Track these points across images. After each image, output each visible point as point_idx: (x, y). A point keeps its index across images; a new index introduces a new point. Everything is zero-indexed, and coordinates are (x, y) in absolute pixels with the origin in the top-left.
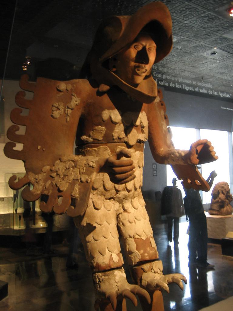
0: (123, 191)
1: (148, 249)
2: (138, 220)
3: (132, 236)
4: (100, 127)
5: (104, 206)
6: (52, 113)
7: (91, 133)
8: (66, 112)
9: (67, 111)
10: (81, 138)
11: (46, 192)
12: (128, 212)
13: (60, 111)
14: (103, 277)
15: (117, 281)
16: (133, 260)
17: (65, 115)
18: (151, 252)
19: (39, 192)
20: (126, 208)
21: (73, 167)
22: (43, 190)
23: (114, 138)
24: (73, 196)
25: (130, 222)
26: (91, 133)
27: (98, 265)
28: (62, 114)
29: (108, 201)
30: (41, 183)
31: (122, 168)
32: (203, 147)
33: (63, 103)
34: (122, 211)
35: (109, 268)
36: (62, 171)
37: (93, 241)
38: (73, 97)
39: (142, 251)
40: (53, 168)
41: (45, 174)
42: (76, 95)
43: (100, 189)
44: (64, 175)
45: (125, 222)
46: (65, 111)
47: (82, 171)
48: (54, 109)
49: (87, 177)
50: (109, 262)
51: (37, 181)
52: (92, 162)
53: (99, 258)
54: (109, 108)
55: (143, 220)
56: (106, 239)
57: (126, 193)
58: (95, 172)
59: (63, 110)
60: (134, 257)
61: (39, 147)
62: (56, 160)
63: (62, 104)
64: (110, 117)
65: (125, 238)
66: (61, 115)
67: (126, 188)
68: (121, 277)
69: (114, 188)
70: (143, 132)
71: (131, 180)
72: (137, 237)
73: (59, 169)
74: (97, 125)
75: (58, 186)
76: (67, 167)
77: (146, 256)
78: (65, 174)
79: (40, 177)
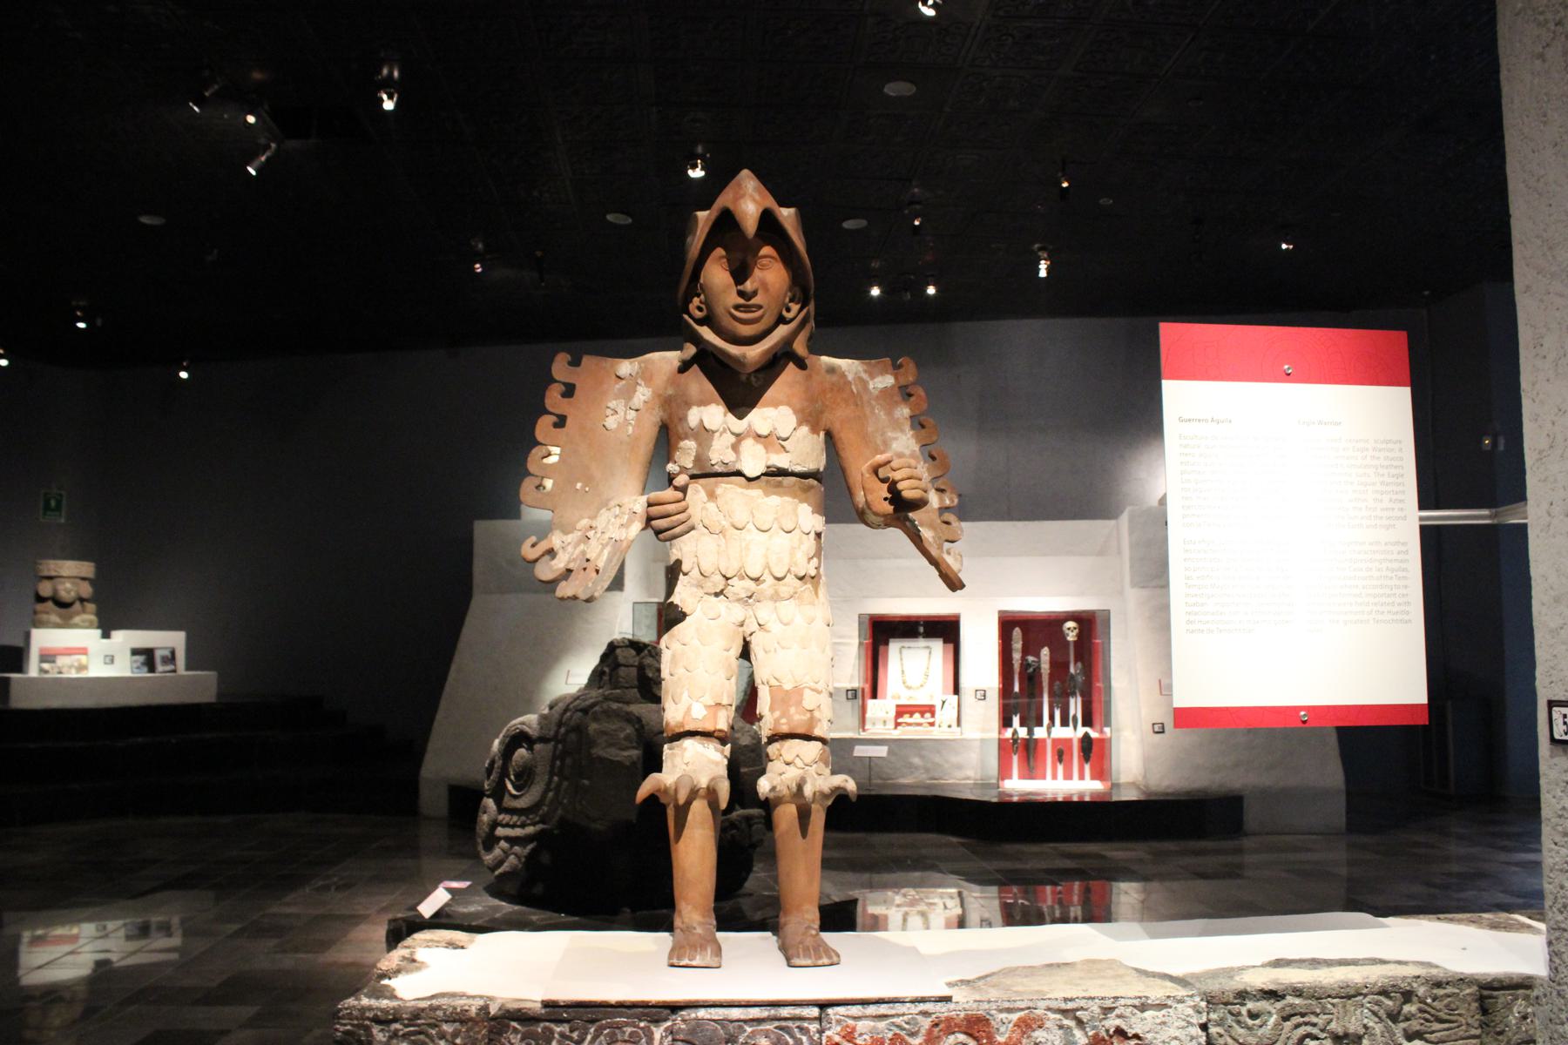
1: (793, 710)
2: (783, 648)
18: (797, 717)
22: (569, 562)
28: (621, 420)
29: (713, 599)
33: (623, 401)
38: (638, 387)
42: (643, 383)
46: (625, 414)
48: (609, 412)
50: (684, 718)
54: (703, 403)
58: (636, 522)
59: (622, 413)
61: (579, 485)
64: (701, 421)
66: (619, 423)
77: (783, 724)
79: (570, 538)
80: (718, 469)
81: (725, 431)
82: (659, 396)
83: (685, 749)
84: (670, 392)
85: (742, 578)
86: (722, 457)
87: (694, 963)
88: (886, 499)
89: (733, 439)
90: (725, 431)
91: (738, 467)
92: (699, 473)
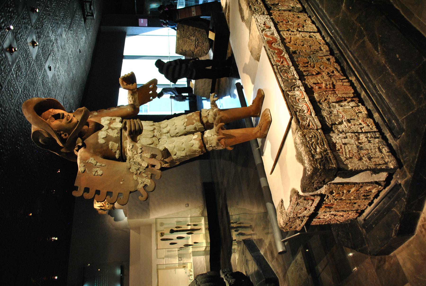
0: (154, 133)
1: (193, 117)
2: (175, 124)
3: (184, 128)
4: (109, 145)
5: (163, 144)
6: (99, 175)
7: (114, 151)
8: (99, 166)
9: (98, 165)
10: (117, 158)
11: (149, 176)
12: (170, 130)
14: (208, 144)
15: (211, 136)
16: (200, 127)
17: (101, 167)
18: (195, 115)
19: (149, 181)
20: (167, 131)
21: (134, 159)
22: (148, 178)
23: (117, 136)
25: (176, 129)
26: (114, 151)
27: (200, 147)
28: (100, 169)
30: (144, 180)
31: (132, 126)
32: (124, 81)
34: (169, 134)
35: (201, 140)
36: (136, 167)
37: (185, 151)
38: (89, 162)
39: (194, 121)
40: (135, 173)
41: (138, 178)
45: (176, 133)
47: (135, 153)
48: (96, 174)
49: (139, 149)
51: (142, 182)
52: (130, 146)
53: (196, 147)
55: (174, 121)
57: (155, 131)
59: (97, 169)
60: (198, 126)
61: (121, 183)
62: (130, 171)
64: (103, 138)
65: (186, 132)
68: (208, 133)
69: (152, 138)
70: (114, 119)
72: (185, 125)
73: (135, 169)
74: (109, 147)
75: (145, 168)
76: (134, 163)
78: (138, 164)
79: (140, 181)
80: (119, 135)
81: (107, 132)
82: (93, 155)
83: (207, 136)
84: (92, 151)
86: (116, 133)
87: (269, 114)
88: (132, 85)
89: (110, 130)
90: (107, 132)
91: (119, 129)
92: (120, 142)
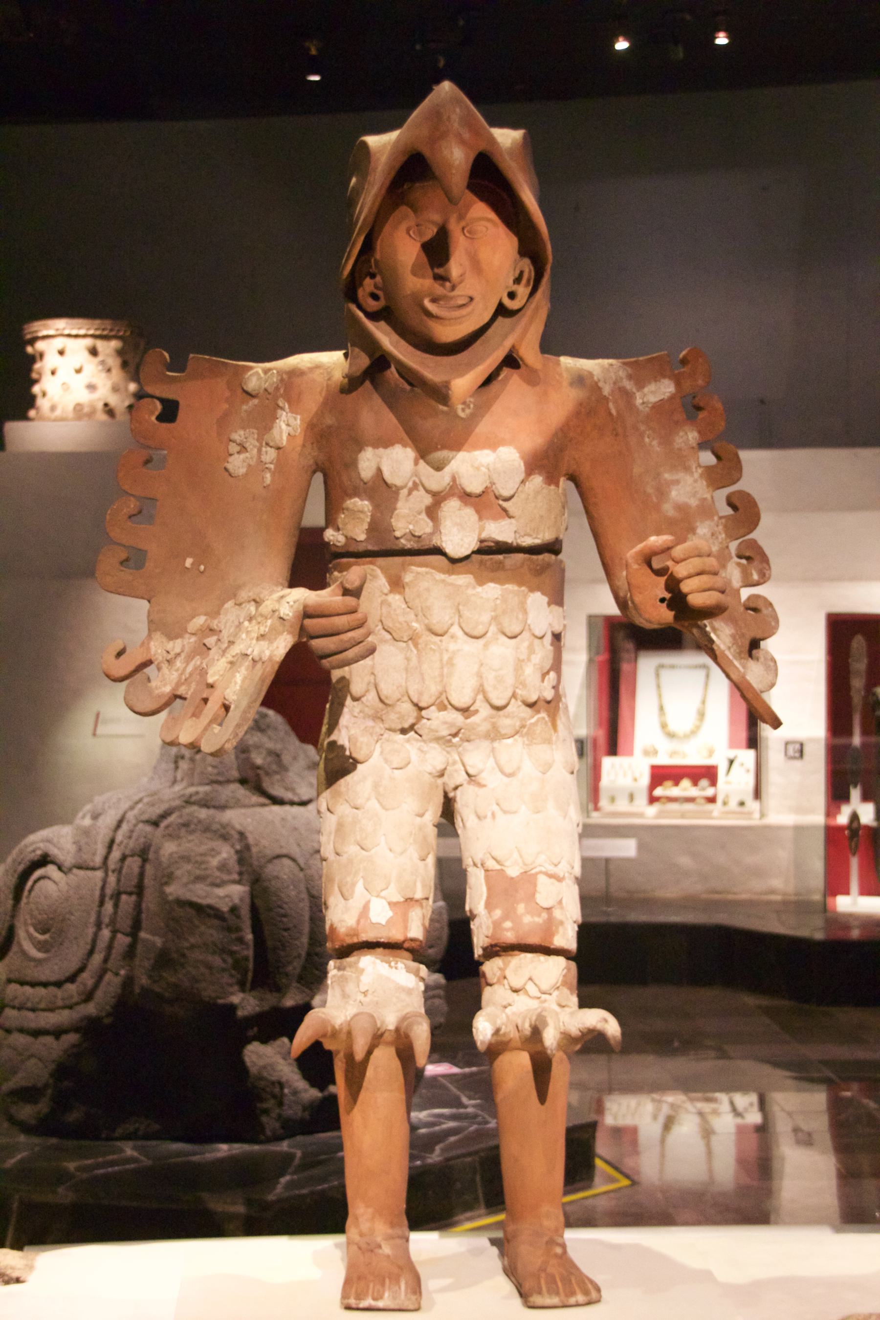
1: (521, 908)
2: (505, 812)
4: (357, 499)
12: (481, 785)
13: (247, 455)
18: (527, 919)
22: (179, 684)
24: (227, 700)
28: (253, 463)
33: (255, 431)
38: (279, 412)
43: (367, 700)
44: (229, 642)
46: (259, 451)
48: (233, 448)
50: (358, 922)
54: (385, 442)
56: (364, 852)
59: (255, 451)
61: (189, 562)
63: (253, 433)
64: (379, 471)
66: (249, 466)
67: (407, 692)
71: (364, 657)
77: (507, 930)
79: (176, 646)
80: (408, 544)
81: (415, 486)
83: (362, 971)
84: (329, 420)
85: (442, 707)
86: (411, 527)
87: (380, 1304)
88: (662, 600)
89: (428, 500)
90: (415, 486)
91: (436, 541)
92: (376, 548)
